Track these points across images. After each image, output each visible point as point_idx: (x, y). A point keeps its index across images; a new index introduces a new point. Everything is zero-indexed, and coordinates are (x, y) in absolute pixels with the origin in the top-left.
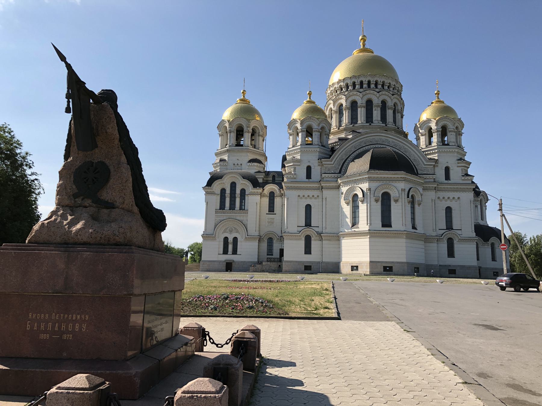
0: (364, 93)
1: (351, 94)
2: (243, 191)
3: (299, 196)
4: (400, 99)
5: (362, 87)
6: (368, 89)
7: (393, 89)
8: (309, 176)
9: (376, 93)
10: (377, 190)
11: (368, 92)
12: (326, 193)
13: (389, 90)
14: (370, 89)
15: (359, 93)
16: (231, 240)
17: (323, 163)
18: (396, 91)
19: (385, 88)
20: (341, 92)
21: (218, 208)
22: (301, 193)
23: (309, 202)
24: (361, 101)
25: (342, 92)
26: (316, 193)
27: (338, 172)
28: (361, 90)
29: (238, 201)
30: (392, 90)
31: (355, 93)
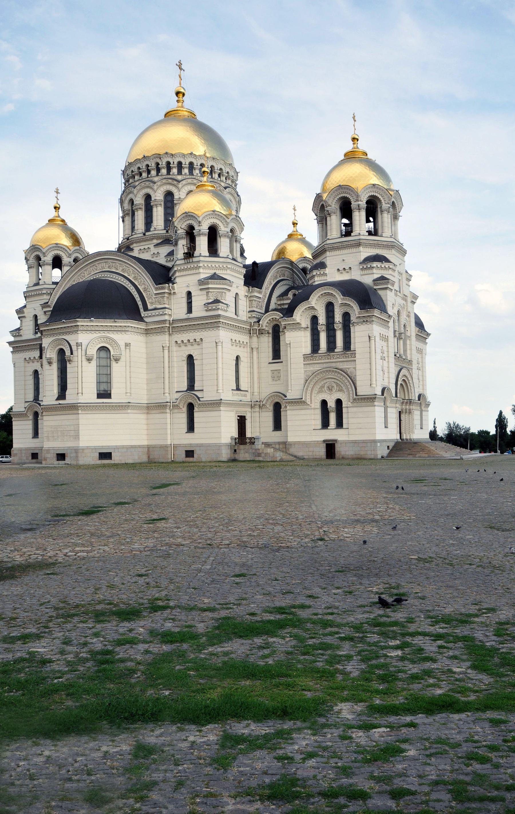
0: (184, 182)
4: (236, 196)
5: (180, 172)
6: (191, 177)
7: (226, 179)
11: (189, 181)
13: (219, 179)
14: (193, 177)
15: (175, 182)
18: (229, 182)
19: (214, 176)
20: (148, 177)
25: (149, 176)
28: (179, 178)
30: (224, 180)
31: (170, 181)
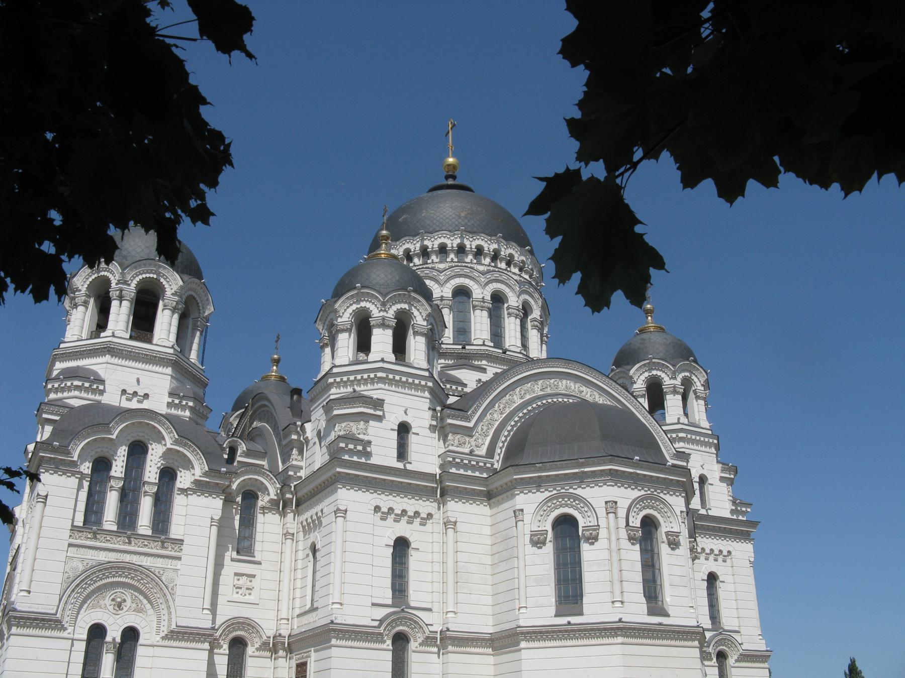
1: (457, 270)
2: (168, 475)
3: (377, 509)
8: (402, 453)
9: (513, 282)
10: (632, 514)
12: (455, 508)
16: (114, 634)
17: (449, 421)
21: (79, 520)
22: (386, 501)
23: (402, 529)
24: (480, 293)
26: (425, 506)
27: (483, 451)
29: (146, 506)
